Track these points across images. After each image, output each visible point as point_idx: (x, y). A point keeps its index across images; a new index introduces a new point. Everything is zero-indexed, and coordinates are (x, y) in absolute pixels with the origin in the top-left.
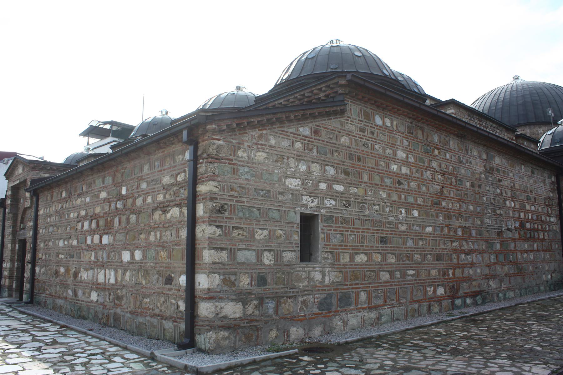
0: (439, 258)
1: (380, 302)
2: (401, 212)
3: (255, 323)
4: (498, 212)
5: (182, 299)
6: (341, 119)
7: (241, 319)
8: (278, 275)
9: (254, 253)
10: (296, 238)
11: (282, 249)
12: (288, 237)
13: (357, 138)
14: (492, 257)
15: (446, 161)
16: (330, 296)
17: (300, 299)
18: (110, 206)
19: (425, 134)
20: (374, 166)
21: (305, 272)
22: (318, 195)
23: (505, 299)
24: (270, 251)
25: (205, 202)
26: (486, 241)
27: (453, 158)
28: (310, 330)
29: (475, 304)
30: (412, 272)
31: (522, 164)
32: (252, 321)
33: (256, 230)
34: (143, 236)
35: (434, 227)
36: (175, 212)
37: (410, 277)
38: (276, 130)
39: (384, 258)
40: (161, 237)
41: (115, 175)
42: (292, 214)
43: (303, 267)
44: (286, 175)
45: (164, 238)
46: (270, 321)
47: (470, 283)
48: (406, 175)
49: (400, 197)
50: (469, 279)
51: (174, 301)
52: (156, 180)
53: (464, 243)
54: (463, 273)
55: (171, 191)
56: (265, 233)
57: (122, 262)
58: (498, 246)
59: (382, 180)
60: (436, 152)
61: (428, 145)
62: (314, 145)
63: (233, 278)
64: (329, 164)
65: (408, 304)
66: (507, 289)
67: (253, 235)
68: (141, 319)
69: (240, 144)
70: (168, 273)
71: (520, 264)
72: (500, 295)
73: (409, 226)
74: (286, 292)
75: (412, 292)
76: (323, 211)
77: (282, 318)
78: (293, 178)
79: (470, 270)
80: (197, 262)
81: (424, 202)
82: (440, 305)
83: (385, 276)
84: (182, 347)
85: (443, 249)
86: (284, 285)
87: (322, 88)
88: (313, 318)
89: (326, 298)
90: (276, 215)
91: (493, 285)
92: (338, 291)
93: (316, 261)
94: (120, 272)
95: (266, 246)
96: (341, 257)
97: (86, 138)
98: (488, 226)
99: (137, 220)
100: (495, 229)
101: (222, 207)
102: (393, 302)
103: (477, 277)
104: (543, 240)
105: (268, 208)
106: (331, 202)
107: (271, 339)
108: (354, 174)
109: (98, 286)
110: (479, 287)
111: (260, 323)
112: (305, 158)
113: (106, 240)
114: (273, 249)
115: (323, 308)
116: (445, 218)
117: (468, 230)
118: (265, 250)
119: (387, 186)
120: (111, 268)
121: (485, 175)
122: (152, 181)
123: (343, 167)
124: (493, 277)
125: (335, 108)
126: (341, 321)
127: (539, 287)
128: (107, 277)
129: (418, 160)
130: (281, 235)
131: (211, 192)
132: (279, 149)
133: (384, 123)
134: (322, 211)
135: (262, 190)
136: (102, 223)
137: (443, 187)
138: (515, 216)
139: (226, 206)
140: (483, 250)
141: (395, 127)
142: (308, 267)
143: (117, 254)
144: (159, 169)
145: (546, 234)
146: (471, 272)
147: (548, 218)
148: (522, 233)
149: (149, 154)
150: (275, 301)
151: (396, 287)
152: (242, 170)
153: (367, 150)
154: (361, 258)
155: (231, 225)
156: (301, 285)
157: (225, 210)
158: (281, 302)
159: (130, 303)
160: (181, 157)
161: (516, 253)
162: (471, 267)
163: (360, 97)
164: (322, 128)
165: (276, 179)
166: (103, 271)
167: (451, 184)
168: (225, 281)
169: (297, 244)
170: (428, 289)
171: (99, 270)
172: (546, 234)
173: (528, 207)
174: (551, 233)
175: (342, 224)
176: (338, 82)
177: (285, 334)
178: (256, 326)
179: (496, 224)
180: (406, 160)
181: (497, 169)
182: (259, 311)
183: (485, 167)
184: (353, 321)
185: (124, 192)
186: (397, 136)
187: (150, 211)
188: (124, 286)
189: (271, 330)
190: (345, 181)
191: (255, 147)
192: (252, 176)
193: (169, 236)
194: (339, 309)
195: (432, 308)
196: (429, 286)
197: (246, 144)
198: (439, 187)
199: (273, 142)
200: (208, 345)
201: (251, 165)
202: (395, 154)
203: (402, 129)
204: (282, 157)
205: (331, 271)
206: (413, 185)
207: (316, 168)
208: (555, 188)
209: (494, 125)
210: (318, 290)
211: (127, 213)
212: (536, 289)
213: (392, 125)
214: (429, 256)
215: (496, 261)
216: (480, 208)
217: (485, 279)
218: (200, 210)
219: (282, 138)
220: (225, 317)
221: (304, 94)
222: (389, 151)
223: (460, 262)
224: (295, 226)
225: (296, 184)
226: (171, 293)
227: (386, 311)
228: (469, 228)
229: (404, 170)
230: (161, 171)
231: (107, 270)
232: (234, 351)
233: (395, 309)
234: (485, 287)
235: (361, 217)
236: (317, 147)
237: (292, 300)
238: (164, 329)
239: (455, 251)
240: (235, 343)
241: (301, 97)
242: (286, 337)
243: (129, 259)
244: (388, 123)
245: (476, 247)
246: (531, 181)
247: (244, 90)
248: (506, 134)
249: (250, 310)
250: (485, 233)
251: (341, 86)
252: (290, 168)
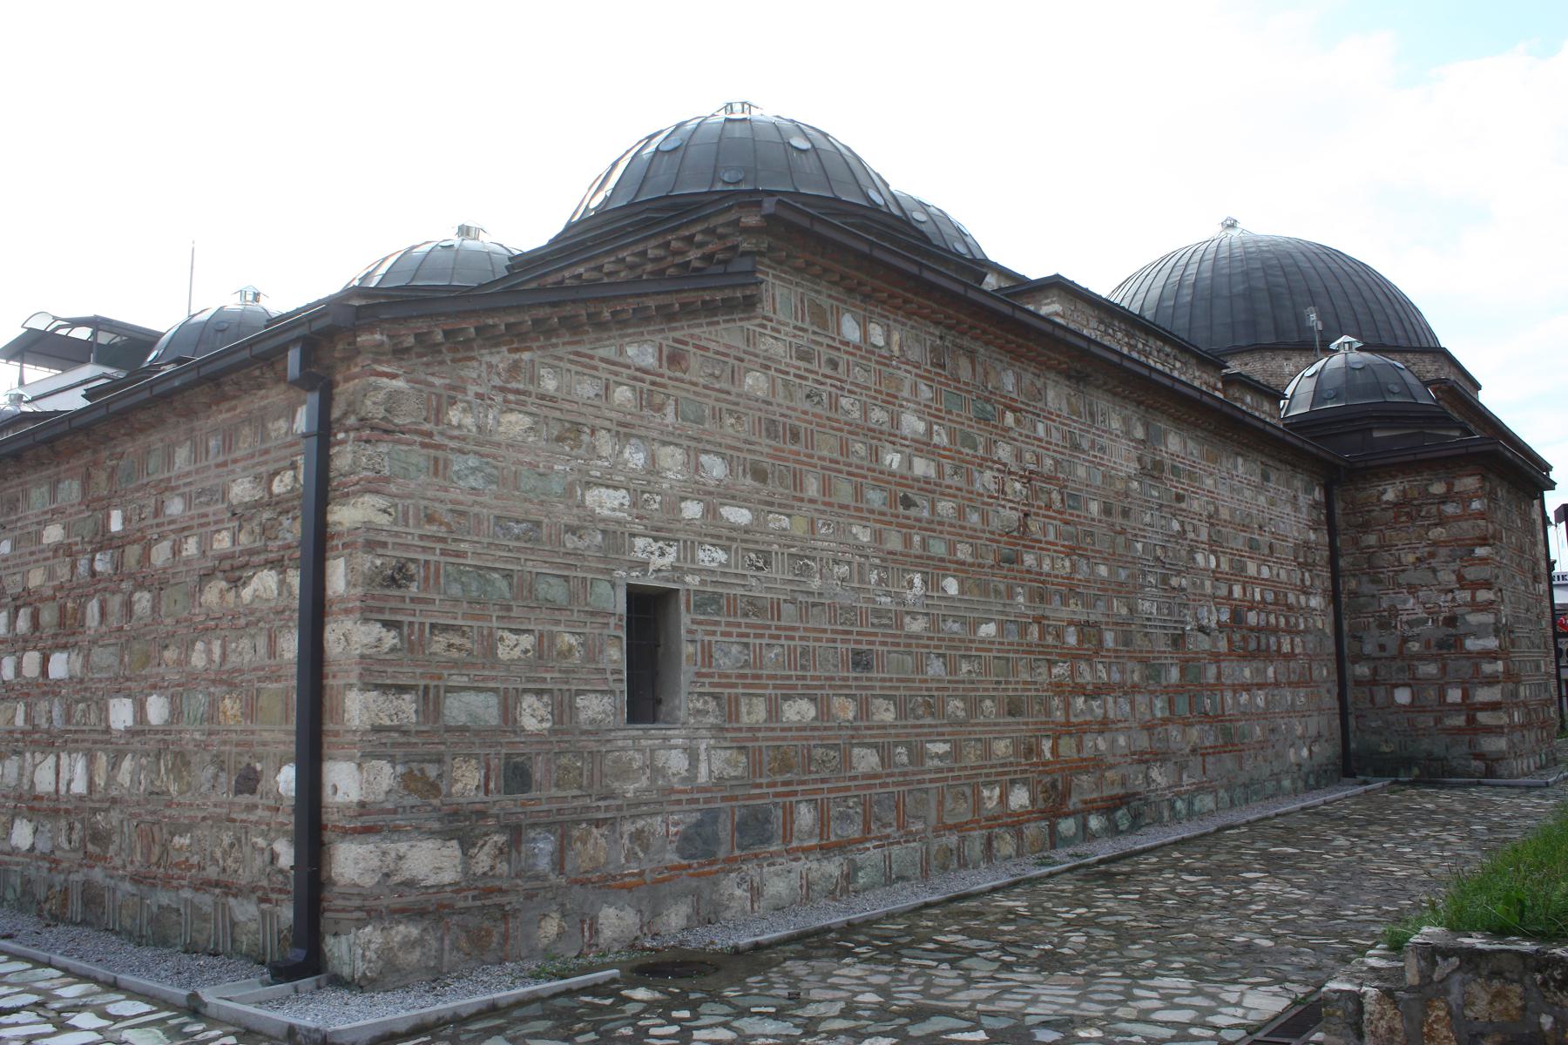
0: (1014, 708)
1: (854, 831)
2: (911, 584)
3: (497, 899)
4: (1174, 582)
5: (285, 833)
6: (746, 324)
7: (457, 888)
8: (564, 761)
9: (493, 700)
10: (616, 655)
11: (574, 688)
12: (592, 653)
13: (791, 378)
14: (1159, 704)
15: (1036, 443)
16: (712, 816)
17: (628, 828)
18: (74, 567)
19: (979, 369)
20: (835, 456)
21: (640, 750)
22: (679, 535)
23: (1191, 814)
24: (539, 693)
25: (351, 555)
26: (1141, 661)
28: (656, 914)
29: (1113, 830)
30: (941, 748)
31: (1238, 454)
32: (489, 892)
33: (500, 633)
34: (170, 655)
35: (1001, 625)
36: (265, 583)
37: (936, 762)
38: (560, 351)
39: (864, 710)
40: (224, 656)
41: (89, 476)
42: (603, 588)
43: (634, 738)
44: (587, 478)
45: (233, 659)
46: (542, 893)
47: (1098, 774)
48: (927, 480)
49: (907, 541)
50: (1097, 764)
51: (261, 842)
52: (211, 491)
53: (1083, 666)
54: (1079, 748)
55: (255, 522)
56: (527, 641)
57: (108, 730)
58: (1174, 674)
59: (858, 493)
60: (1010, 418)
61: (988, 400)
62: (668, 396)
63: (432, 771)
64: (708, 447)
65: (930, 835)
66: (1197, 790)
67: (491, 650)
68: (164, 898)
69: (454, 388)
70: (246, 759)
71: (1231, 721)
72: (1179, 805)
73: (934, 621)
74: (588, 808)
75: (941, 803)
76: (692, 581)
77: (576, 882)
78: (608, 487)
79: (1100, 741)
80: (329, 726)
81: (974, 554)
82: (1019, 835)
83: (866, 760)
84: (283, 972)
85: (1025, 683)
86: (580, 787)
87: (693, 236)
88: (663, 880)
89: (699, 824)
90: (557, 592)
91: (1159, 779)
92: (734, 803)
93: (672, 721)
94: (102, 760)
95: (529, 680)
96: (744, 709)
97: (14, 367)
98: (1149, 619)
99: (155, 608)
100: (1165, 628)
101: (401, 568)
102: (889, 831)
103: (1118, 759)
104: (1291, 656)
105: (535, 570)
106: (714, 555)
107: (546, 941)
108: (781, 478)
109: (36, 804)
110: (1123, 784)
111: (512, 898)
112: (643, 432)
113: (59, 666)
114: (549, 686)
115: (694, 851)
116: (1031, 599)
117: (1093, 631)
118: (525, 691)
119: (872, 512)
120: (77, 751)
121: (1140, 483)
122: (199, 494)
123: (749, 457)
124: (1159, 756)
125: (728, 293)
126: (745, 886)
127: (1279, 781)
128: (64, 776)
129: (958, 442)
130: (571, 648)
131: (369, 526)
132: (567, 406)
133: (865, 335)
134: (688, 579)
135: (518, 522)
136: (48, 616)
137: (1026, 515)
138: (1219, 593)
139: (412, 567)
140: (1134, 686)
141: (896, 348)
142: (648, 736)
143: (93, 707)
144: (221, 459)
145: (1298, 640)
146: (1102, 744)
147: (1303, 599)
148: (1237, 637)
149: (190, 413)
150: (554, 834)
151: (895, 789)
152: (458, 464)
153: (818, 410)
154: (799, 711)
155: (428, 621)
156: (631, 789)
157: (411, 578)
158: (571, 837)
159: (132, 850)
160: (282, 424)
161: (1222, 691)
162: (1101, 732)
163: (800, 262)
164: (690, 348)
165: (557, 488)
166: (51, 760)
167: (1048, 507)
168: (409, 781)
169: (619, 672)
170: (986, 793)
171: (38, 756)
172: (1298, 640)
173: (1252, 569)
174: (1310, 637)
175: (746, 615)
176: (738, 220)
177: (586, 927)
178: (501, 907)
179: (1168, 615)
180: (925, 439)
181: (1174, 467)
182: (509, 863)
183: (1139, 460)
184: (778, 886)
185: (116, 524)
186: (901, 373)
187: (192, 580)
188: (114, 801)
189: (545, 916)
190: (756, 496)
191: (499, 399)
192: (490, 479)
193: (246, 652)
194: (737, 853)
195: (995, 844)
196: (986, 784)
197: (473, 389)
198: (1015, 515)
199: (550, 384)
200: (361, 966)
201: (486, 450)
202: (895, 422)
203: (914, 354)
204: (577, 428)
205: (714, 748)
206: (946, 507)
207: (672, 460)
208: (1322, 517)
209: (1168, 349)
210: (679, 802)
211: (123, 585)
212: (1270, 786)
213: (888, 343)
214: (988, 703)
215: (1167, 714)
216: (1127, 572)
217: (1140, 762)
218: (338, 578)
219: (577, 373)
220: (410, 884)
221: (644, 253)
222: (878, 415)
223: (1073, 719)
224: (612, 621)
225: (616, 503)
226: (253, 818)
227: (871, 856)
228: (1095, 625)
229: (921, 467)
230: (224, 464)
231: (64, 756)
232: (436, 978)
234: (1138, 783)
235: (800, 598)
236: (676, 401)
237: (604, 830)
238: (234, 924)
239: (1058, 687)
240: (440, 957)
241: (637, 260)
242: (587, 934)
243: (130, 723)
244: (877, 336)
245: (1116, 677)
246: (1262, 499)
247: (482, 236)
248: (1197, 374)
249: (483, 860)
250: (1139, 640)
251: (748, 231)
252: (600, 458)
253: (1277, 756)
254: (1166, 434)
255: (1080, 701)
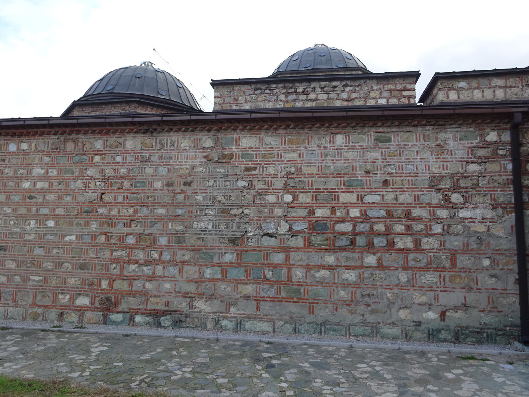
2: (29, 224)
4: (234, 212)
27: (129, 159)
30: (37, 278)
35: (79, 237)
37: (35, 283)
50: (144, 294)
53: (137, 252)
60: (97, 158)
65: (27, 306)
75: (35, 296)
91: (204, 307)
102: (9, 302)
116: (101, 225)
124: (210, 298)
141: (33, 149)
151: (12, 289)
180: (45, 175)
183: (205, 157)
186: (34, 156)
195: (65, 316)
202: (29, 172)
206: (51, 197)
209: (334, 83)
213: (30, 146)
214: (66, 264)
215: (219, 276)
223: (125, 273)
228: (150, 234)
229: (40, 185)
233: (10, 309)
239: (117, 260)
246: (376, 154)
248: (375, 88)
250: (191, 241)
253: (373, 312)
254: (238, 140)
255: (133, 267)
